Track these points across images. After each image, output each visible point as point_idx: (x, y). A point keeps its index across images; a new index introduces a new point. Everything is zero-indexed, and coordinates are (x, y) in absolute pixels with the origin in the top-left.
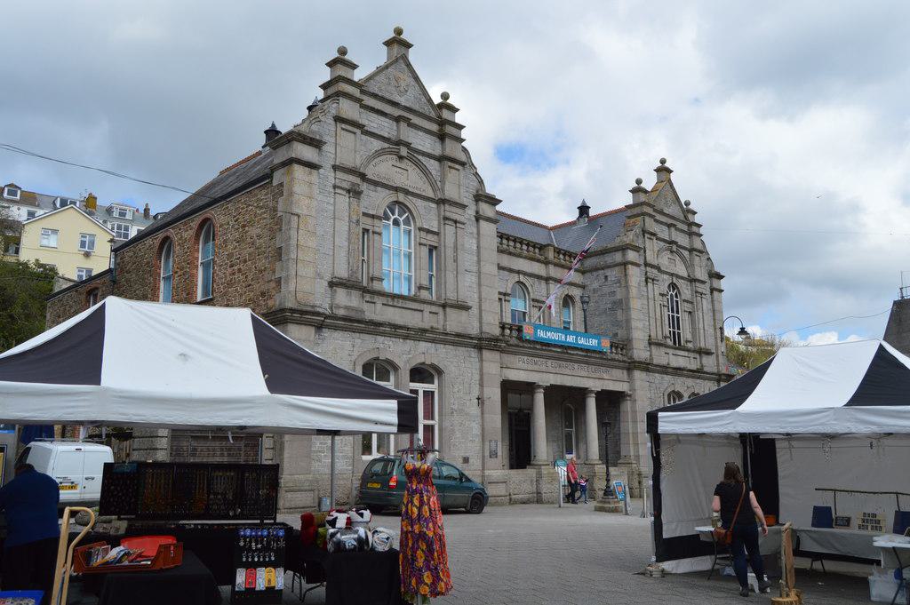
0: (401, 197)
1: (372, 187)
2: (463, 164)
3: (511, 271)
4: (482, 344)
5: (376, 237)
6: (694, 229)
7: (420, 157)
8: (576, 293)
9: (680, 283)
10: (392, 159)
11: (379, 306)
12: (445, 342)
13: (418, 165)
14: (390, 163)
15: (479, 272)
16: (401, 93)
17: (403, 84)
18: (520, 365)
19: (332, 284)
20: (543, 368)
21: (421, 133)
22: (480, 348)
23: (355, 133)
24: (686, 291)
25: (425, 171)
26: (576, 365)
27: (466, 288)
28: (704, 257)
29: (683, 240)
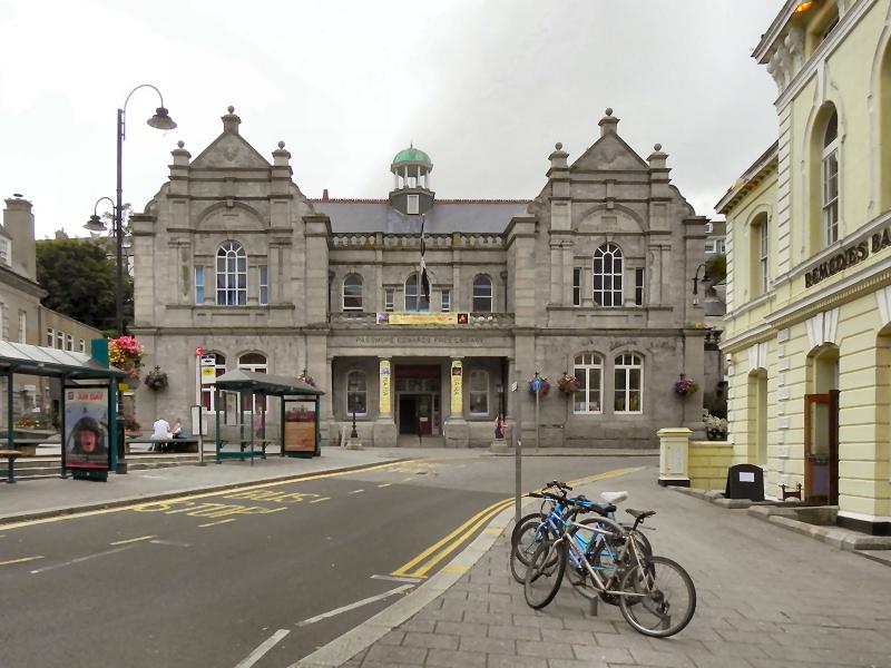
0: (230, 237)
1: (205, 235)
2: (290, 197)
3: (405, 264)
4: (306, 332)
5: (209, 270)
6: (655, 176)
7: (246, 203)
8: (494, 272)
9: (622, 243)
10: (223, 211)
11: (209, 316)
12: (271, 334)
13: (247, 208)
14: (221, 214)
15: (306, 278)
16: (231, 159)
17: (230, 150)
18: (359, 343)
19: (168, 307)
20: (387, 343)
21: (250, 184)
22: (305, 335)
23: (184, 202)
24: (631, 248)
25: (254, 212)
26: (432, 339)
27: (292, 291)
28: (673, 207)
29: (639, 192)
